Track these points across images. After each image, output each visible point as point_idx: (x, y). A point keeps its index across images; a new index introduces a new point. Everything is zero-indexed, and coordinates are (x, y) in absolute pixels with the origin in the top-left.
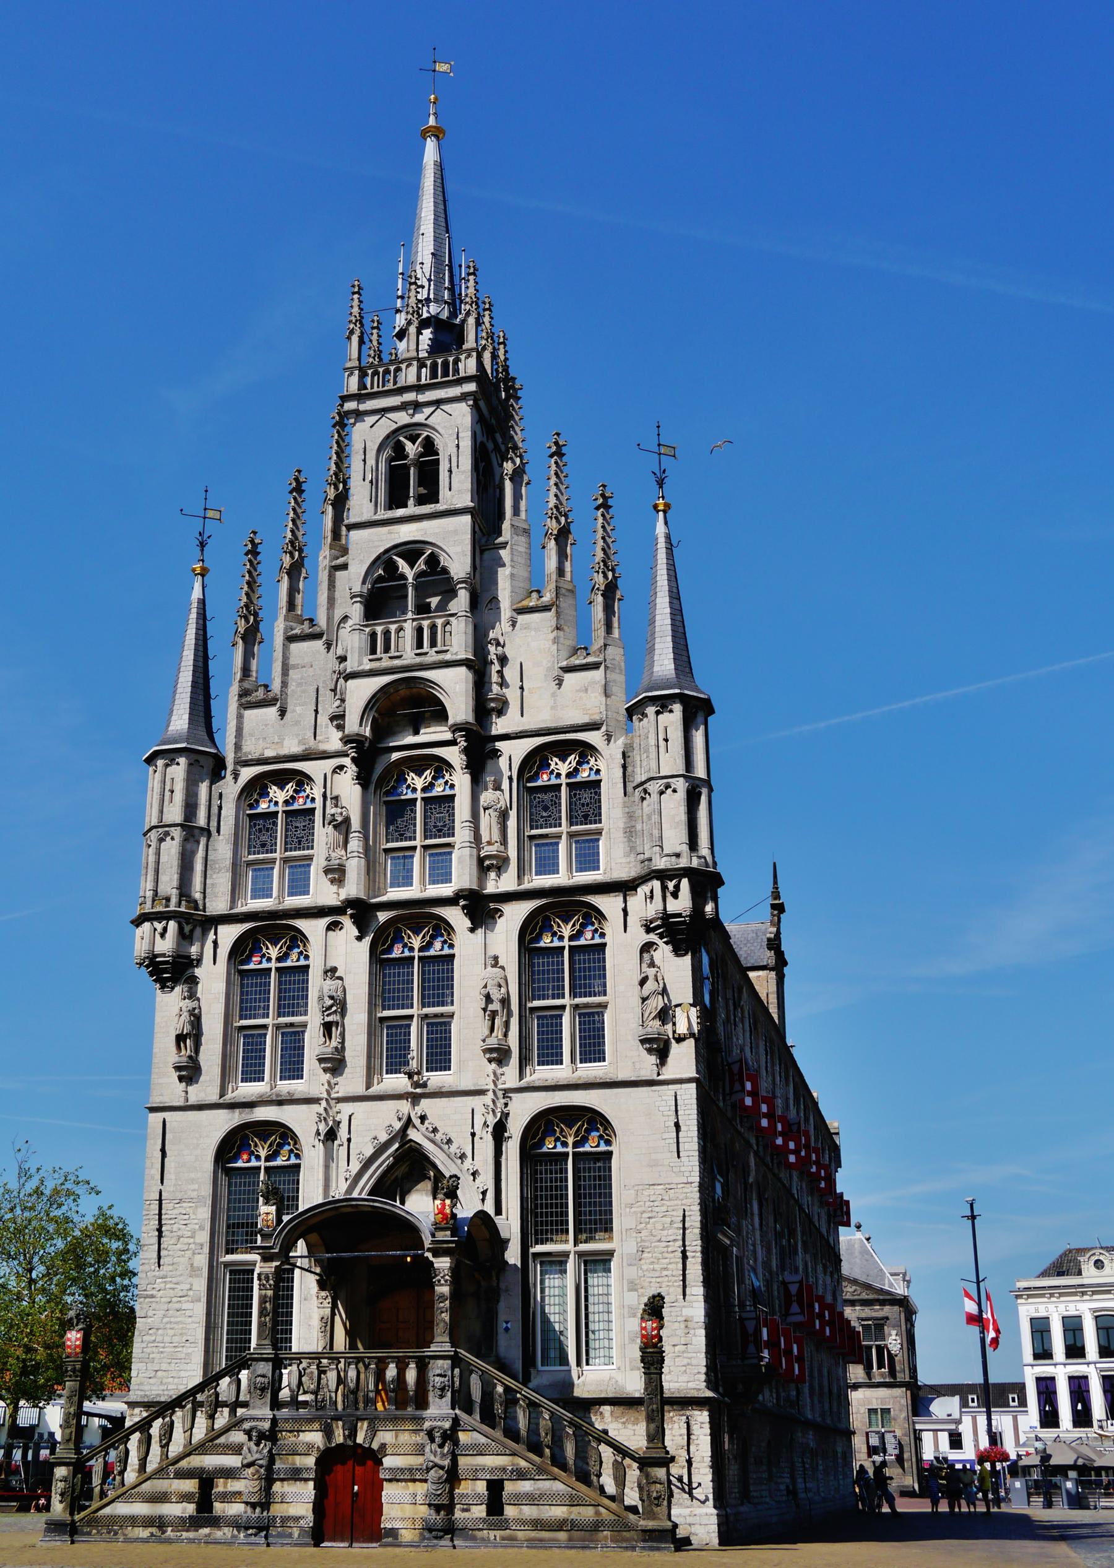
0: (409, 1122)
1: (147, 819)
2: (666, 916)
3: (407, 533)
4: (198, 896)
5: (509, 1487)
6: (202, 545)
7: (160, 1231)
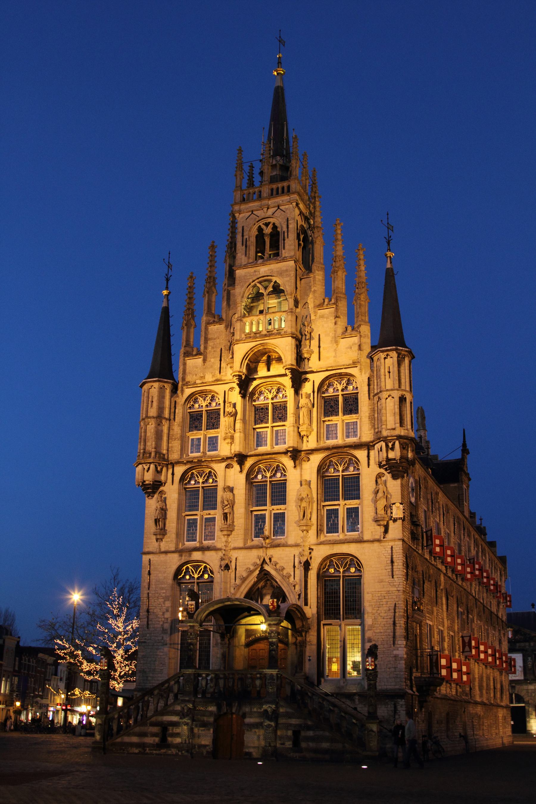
0: (264, 559)
1: (141, 415)
2: (388, 460)
4: (165, 452)
5: (303, 734)
6: (168, 280)
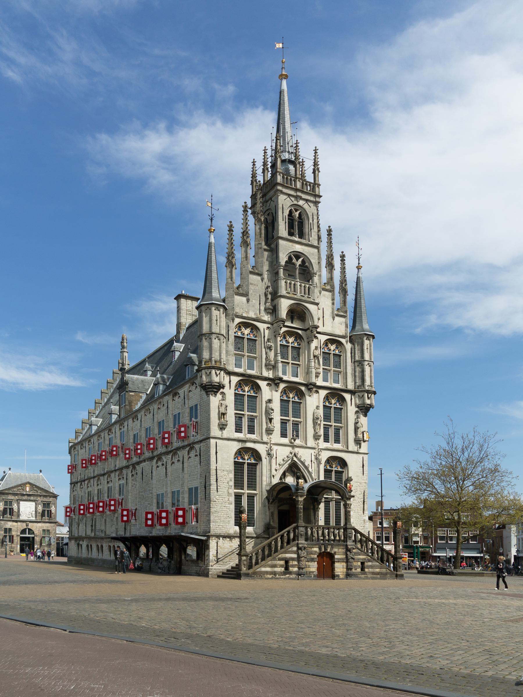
7: (217, 480)
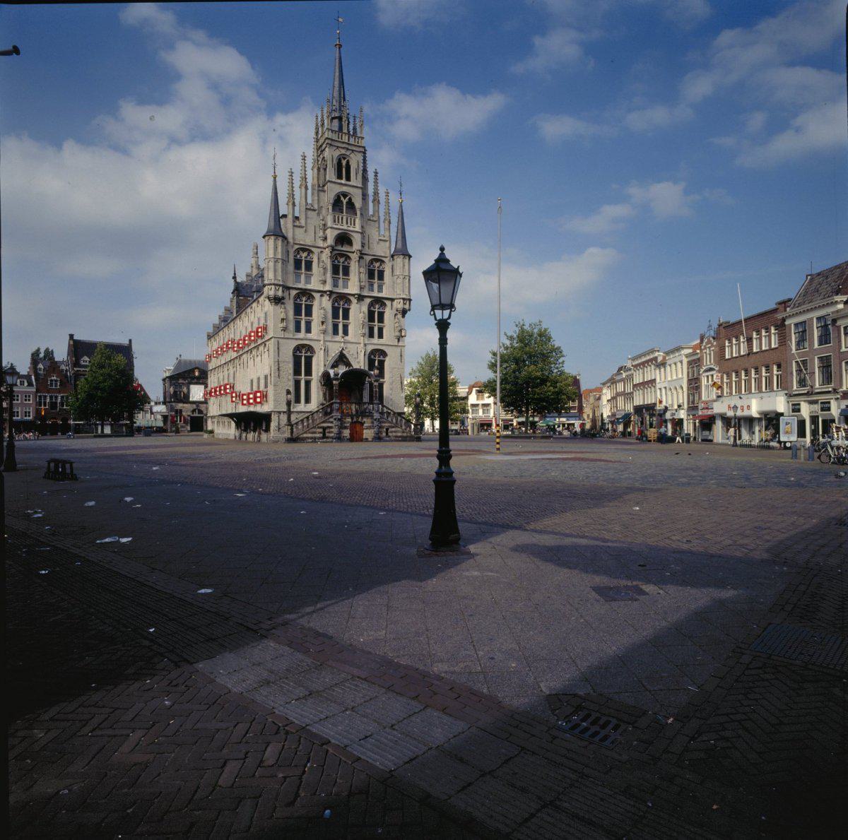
0: (343, 349)
2: (404, 308)
3: (345, 189)
5: (390, 430)
